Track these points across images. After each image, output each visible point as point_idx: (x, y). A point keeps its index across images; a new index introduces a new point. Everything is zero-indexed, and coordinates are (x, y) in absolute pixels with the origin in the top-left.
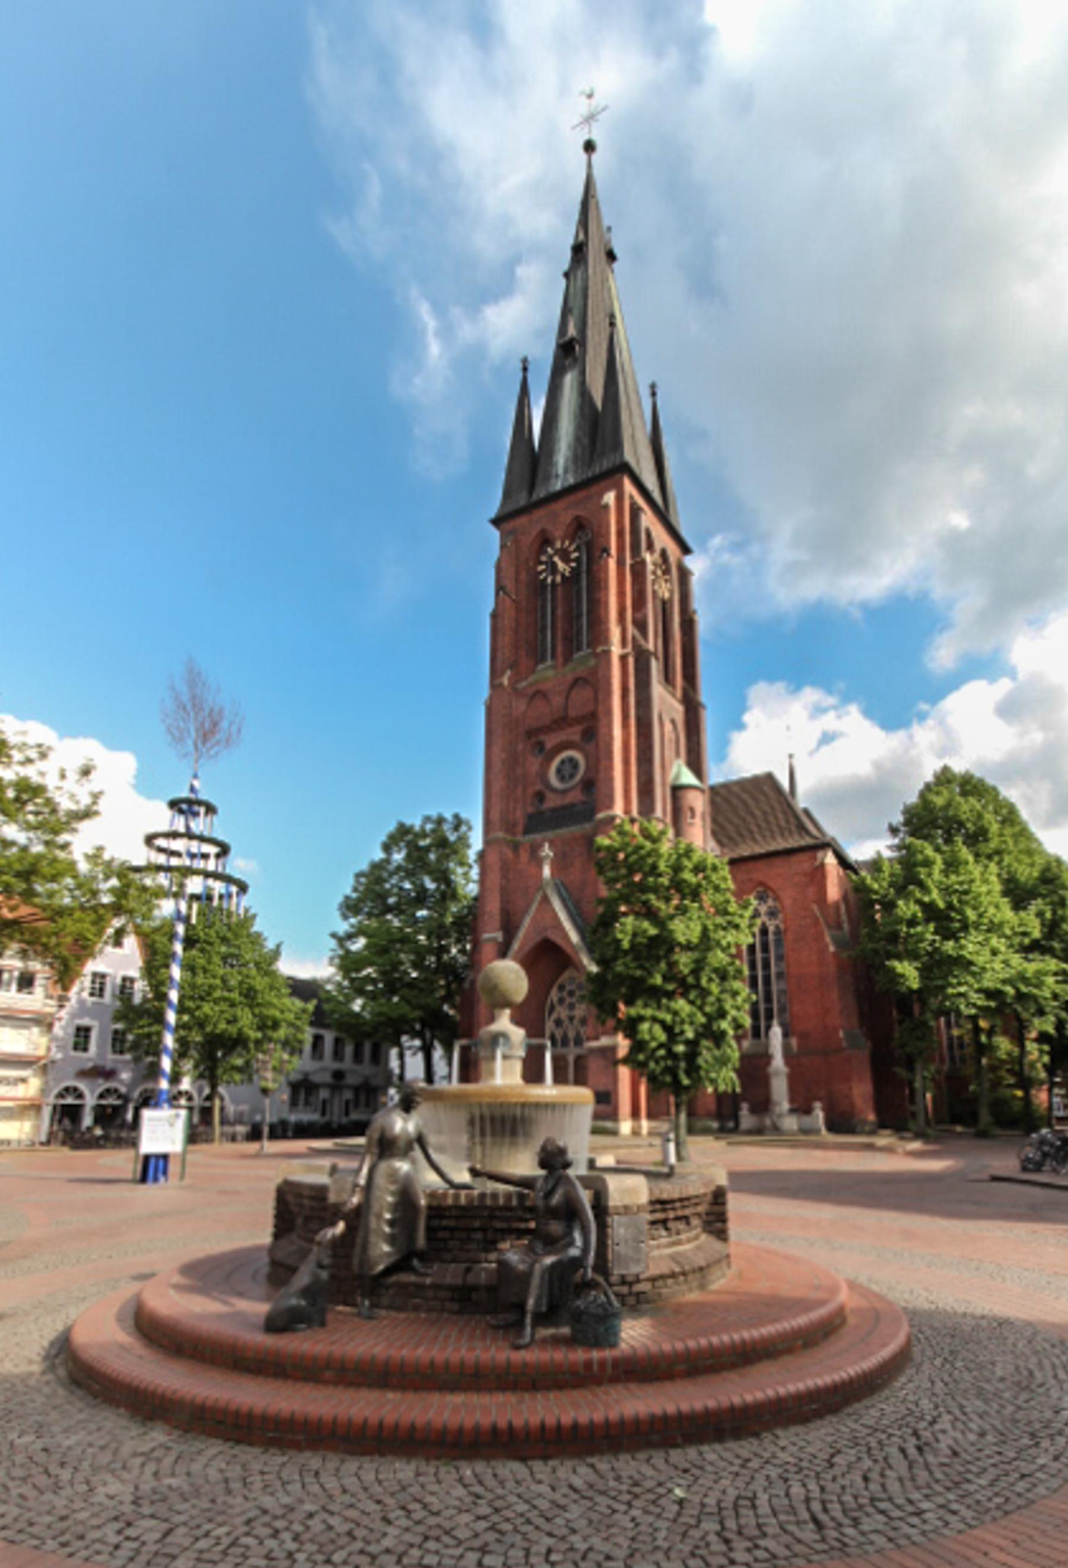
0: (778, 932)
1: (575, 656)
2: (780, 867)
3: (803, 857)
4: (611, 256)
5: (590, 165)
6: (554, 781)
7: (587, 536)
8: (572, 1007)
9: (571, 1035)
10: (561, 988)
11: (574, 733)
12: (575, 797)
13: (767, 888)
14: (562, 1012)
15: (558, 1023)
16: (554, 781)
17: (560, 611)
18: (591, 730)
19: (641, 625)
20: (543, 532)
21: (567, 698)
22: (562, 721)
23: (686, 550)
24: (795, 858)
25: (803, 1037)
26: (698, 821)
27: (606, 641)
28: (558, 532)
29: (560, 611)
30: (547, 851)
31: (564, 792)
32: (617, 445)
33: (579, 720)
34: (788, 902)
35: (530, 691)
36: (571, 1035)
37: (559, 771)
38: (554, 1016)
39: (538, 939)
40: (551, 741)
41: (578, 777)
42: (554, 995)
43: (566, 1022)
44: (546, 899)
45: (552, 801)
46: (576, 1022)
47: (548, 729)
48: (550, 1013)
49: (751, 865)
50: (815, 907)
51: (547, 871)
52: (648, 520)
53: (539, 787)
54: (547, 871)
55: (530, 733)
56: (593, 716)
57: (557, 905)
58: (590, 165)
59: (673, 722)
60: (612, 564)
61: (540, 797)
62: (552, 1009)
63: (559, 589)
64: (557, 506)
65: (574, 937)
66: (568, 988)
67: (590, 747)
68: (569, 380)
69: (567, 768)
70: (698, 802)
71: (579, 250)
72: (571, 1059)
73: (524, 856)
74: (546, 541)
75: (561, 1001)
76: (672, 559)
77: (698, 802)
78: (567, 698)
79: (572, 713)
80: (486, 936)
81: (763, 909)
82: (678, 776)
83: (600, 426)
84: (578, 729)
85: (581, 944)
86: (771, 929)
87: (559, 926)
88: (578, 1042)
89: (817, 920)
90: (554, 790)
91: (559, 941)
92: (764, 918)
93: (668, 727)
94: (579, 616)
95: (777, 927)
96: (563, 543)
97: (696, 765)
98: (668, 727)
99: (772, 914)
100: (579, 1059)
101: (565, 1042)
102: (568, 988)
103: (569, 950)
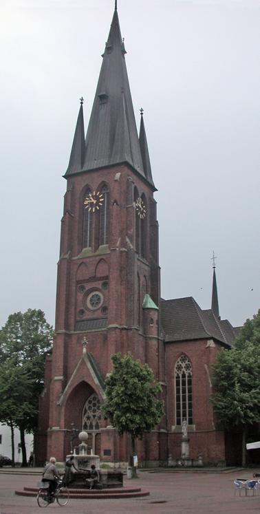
1: (101, 247)
2: (191, 346)
3: (202, 342)
5: (116, 8)
6: (89, 306)
8: (94, 411)
9: (94, 424)
10: (90, 402)
11: (99, 284)
12: (99, 314)
13: (186, 356)
14: (90, 414)
15: (88, 418)
16: (89, 306)
17: (94, 226)
20: (87, 185)
21: (96, 267)
22: (94, 279)
24: (198, 343)
25: (198, 424)
28: (94, 187)
29: (94, 226)
31: (94, 311)
33: (101, 279)
34: (194, 363)
35: (79, 262)
36: (94, 424)
37: (91, 300)
38: (86, 415)
39: (80, 381)
40: (88, 286)
41: (101, 304)
42: (87, 405)
43: (92, 418)
44: (83, 363)
45: (87, 316)
46: (96, 418)
47: (88, 281)
48: (84, 414)
49: (179, 345)
50: (206, 366)
51: (85, 350)
53: (82, 308)
54: (85, 350)
55: (78, 282)
57: (89, 365)
58: (116, 8)
59: (145, 276)
61: (82, 312)
62: (86, 411)
63: (94, 217)
64: (95, 175)
65: (97, 381)
66: (93, 402)
67: (106, 292)
69: (95, 298)
72: (94, 435)
73: (74, 341)
74: (88, 189)
75: (90, 408)
76: (147, 196)
77: (155, 316)
78: (96, 267)
79: (98, 275)
80: (56, 378)
81: (183, 365)
82: (146, 303)
84: (101, 282)
85: (99, 384)
86: (187, 375)
87: (90, 375)
88: (97, 427)
89: (206, 373)
90: (89, 310)
91: (90, 383)
92: (184, 369)
93: (142, 279)
94: (102, 228)
95: (189, 374)
96: (96, 193)
98: (142, 279)
99: (187, 367)
100: (97, 434)
101: (91, 427)
102: (93, 402)
103: (94, 387)
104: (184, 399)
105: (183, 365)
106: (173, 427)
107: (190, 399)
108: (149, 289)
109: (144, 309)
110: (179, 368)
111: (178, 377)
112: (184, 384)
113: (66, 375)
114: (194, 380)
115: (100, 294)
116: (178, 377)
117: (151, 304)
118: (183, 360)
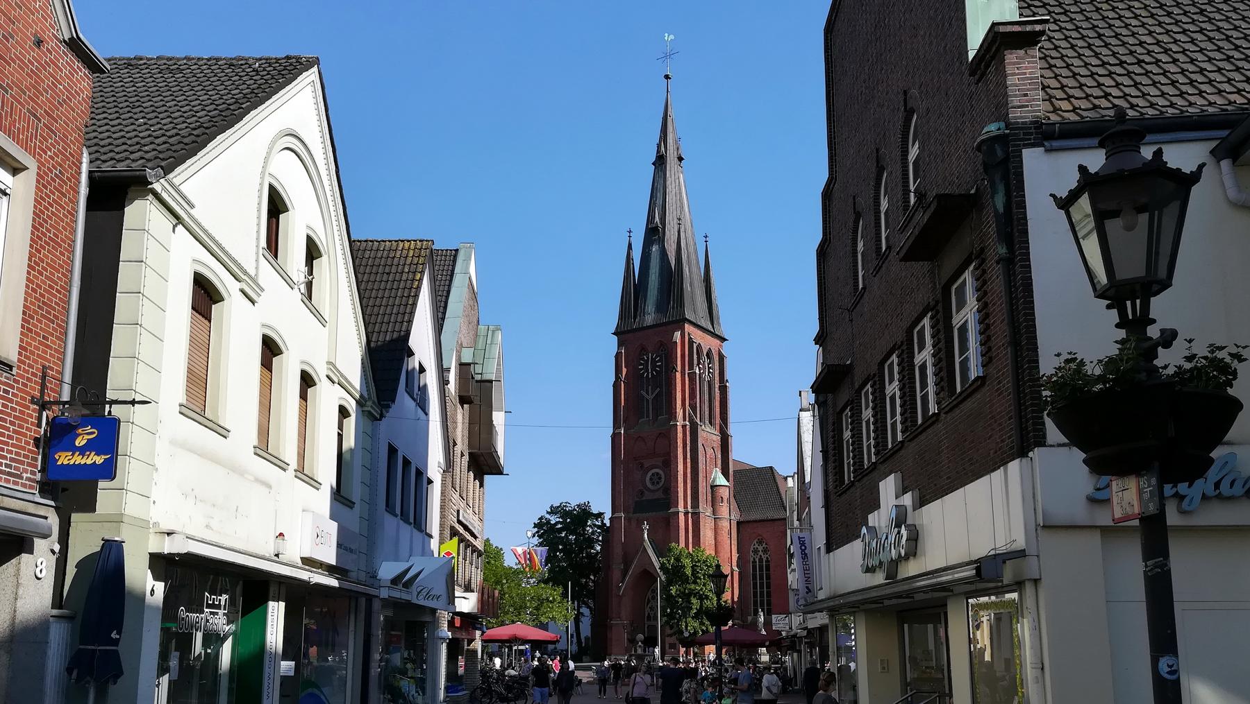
0: (767, 561)
4: (680, 159)
6: (649, 485)
7: (667, 351)
12: (659, 495)
18: (668, 463)
19: (693, 407)
23: (723, 340)
26: (725, 504)
27: (675, 419)
30: (646, 526)
31: (653, 491)
32: (681, 303)
45: (648, 496)
52: (699, 337)
56: (669, 454)
60: (678, 375)
61: (642, 493)
68: (655, 248)
70: (725, 493)
71: (660, 161)
74: (643, 350)
77: (725, 493)
81: (760, 548)
83: (672, 280)
90: (649, 490)
97: (725, 473)
99: (765, 551)
104: (762, 587)
105: (760, 548)
106: (750, 618)
107: (768, 587)
108: (719, 462)
109: (713, 487)
110: (756, 551)
111: (754, 562)
112: (761, 569)
113: (627, 564)
114: (772, 565)
115: (661, 472)
116: (754, 562)
117: (721, 480)
118: (760, 543)
